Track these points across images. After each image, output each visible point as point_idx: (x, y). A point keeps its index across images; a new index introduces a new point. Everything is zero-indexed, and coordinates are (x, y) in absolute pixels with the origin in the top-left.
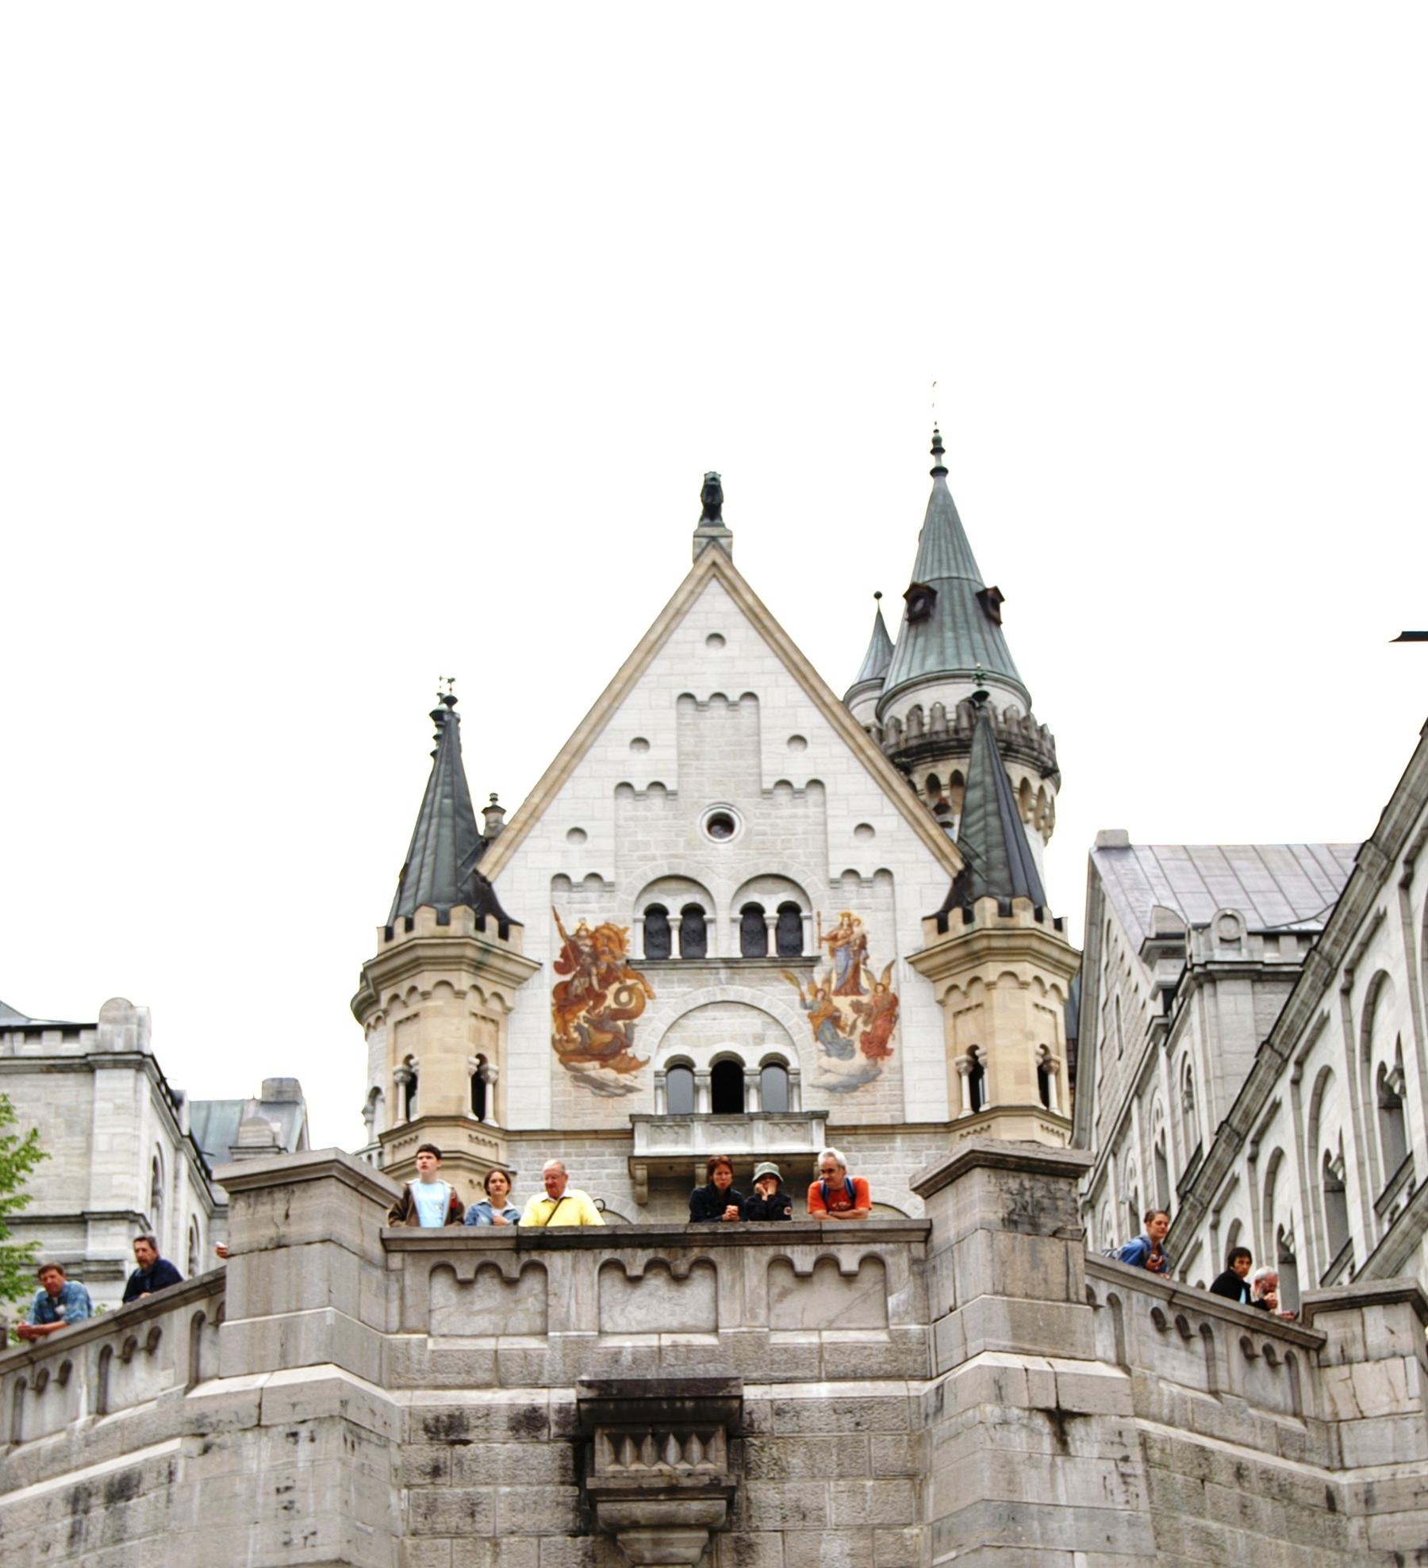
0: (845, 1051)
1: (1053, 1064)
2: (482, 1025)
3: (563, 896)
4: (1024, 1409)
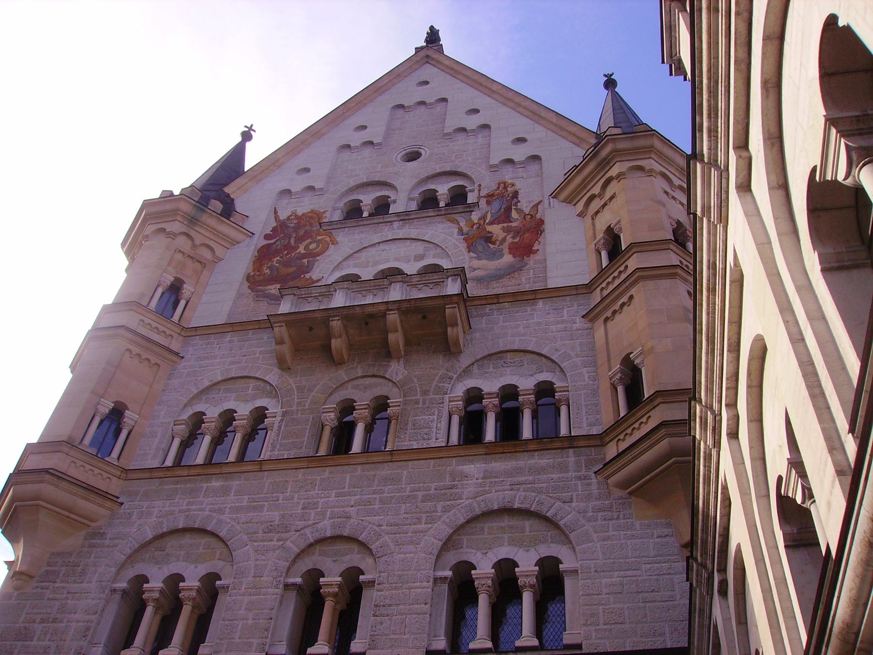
0: (496, 255)
2: (189, 262)
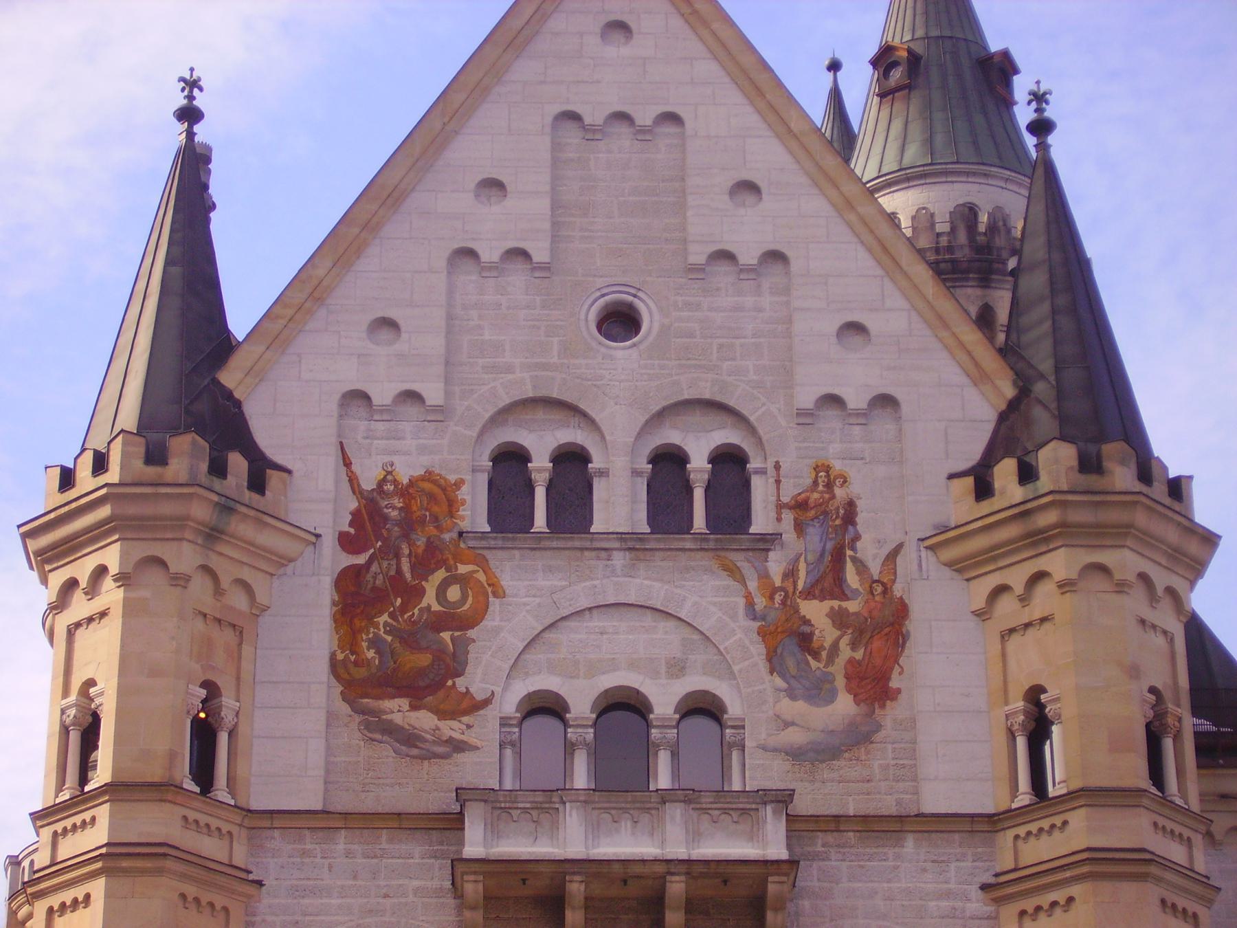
0: (819, 692)
1: (1170, 720)
3: (359, 425)
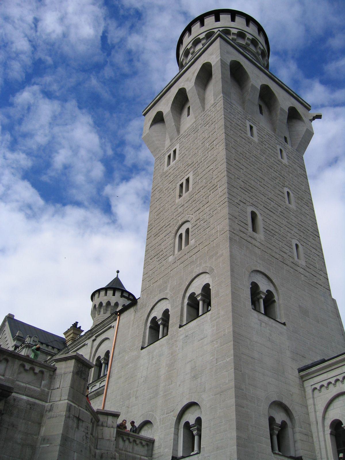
4: (73, 415)
